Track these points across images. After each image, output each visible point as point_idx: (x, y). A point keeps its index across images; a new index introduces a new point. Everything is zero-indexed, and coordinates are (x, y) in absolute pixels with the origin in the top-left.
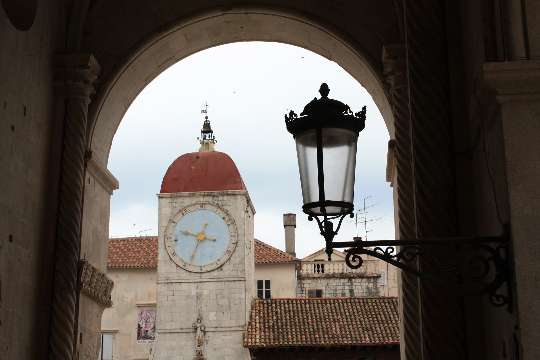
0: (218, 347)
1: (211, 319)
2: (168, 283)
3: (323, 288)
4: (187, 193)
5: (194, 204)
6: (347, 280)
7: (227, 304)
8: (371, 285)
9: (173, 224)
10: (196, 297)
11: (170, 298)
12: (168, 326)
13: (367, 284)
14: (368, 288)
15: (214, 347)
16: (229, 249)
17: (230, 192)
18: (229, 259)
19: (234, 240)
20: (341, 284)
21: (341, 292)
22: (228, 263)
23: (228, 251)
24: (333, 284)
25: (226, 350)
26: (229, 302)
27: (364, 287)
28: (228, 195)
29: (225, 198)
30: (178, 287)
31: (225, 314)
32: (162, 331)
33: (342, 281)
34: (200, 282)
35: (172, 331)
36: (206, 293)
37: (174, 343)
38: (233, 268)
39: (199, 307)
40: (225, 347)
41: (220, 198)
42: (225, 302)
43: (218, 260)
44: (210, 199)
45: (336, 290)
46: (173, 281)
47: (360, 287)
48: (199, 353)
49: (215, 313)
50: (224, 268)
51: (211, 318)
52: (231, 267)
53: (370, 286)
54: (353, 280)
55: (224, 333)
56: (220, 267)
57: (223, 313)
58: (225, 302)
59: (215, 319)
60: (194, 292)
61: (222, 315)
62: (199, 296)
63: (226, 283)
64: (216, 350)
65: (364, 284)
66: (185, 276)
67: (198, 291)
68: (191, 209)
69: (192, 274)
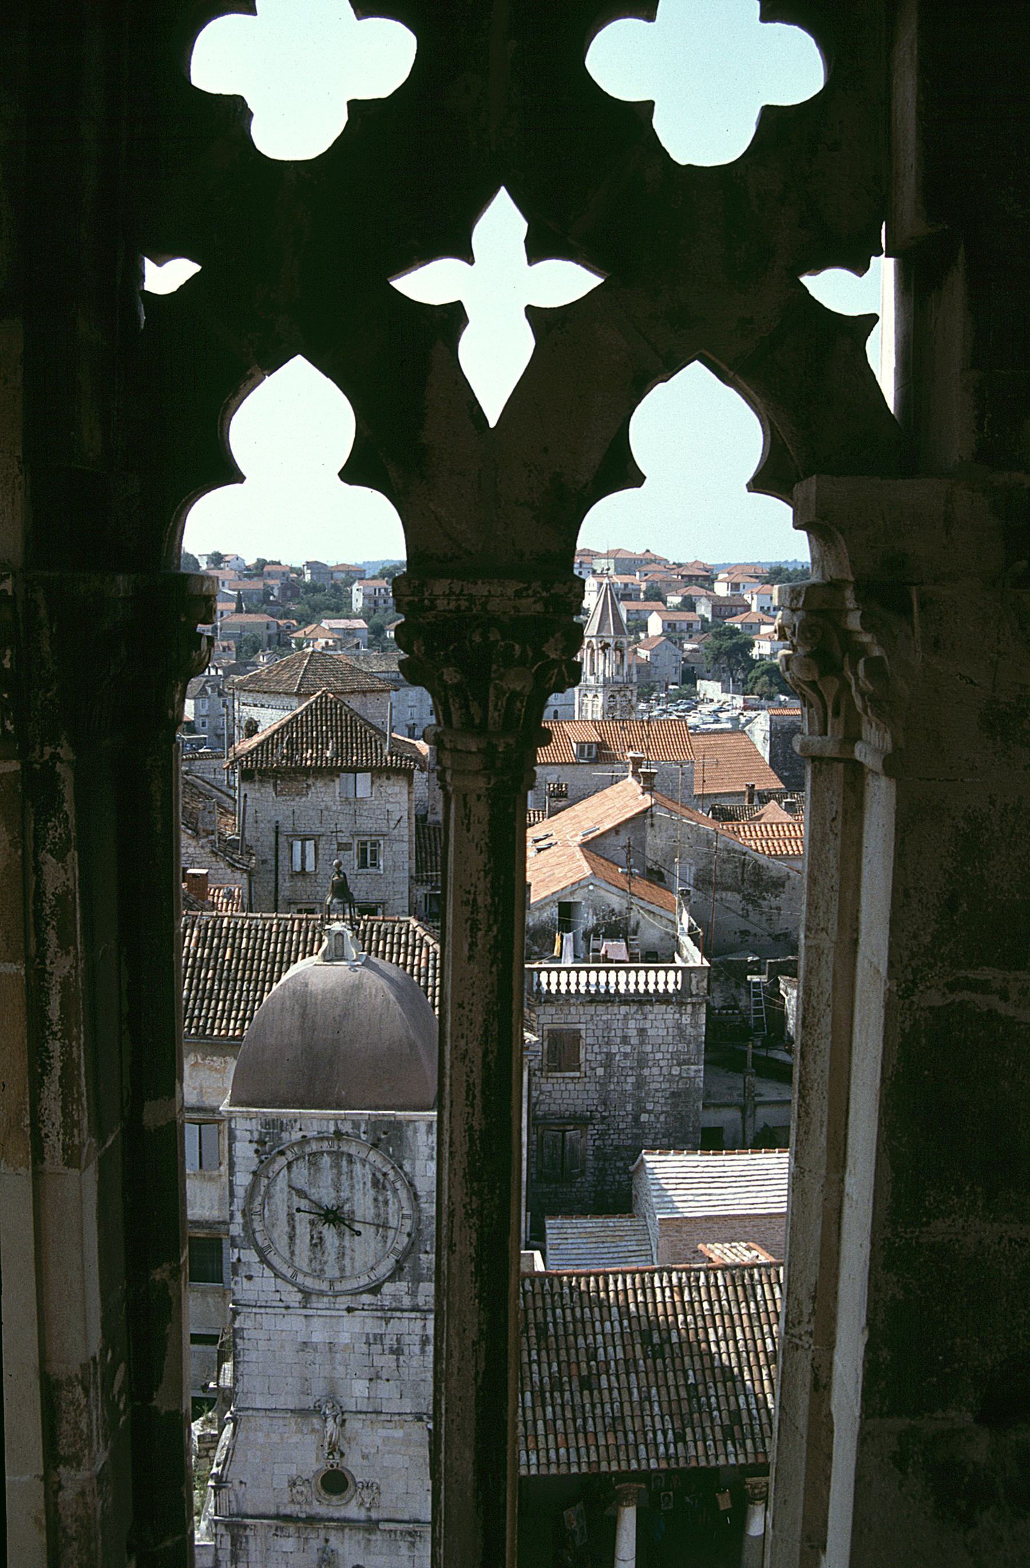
3: (582, 1026)
6: (634, 1008)
8: (686, 1020)
13: (677, 1016)
14: (679, 1027)
15: (364, 1450)
20: (622, 1017)
21: (619, 1033)
24: (604, 1018)
27: (670, 1023)
33: (624, 1009)
43: (372, 1269)
45: (609, 1029)
47: (660, 1024)
50: (388, 1288)
53: (684, 1022)
54: (648, 1008)
56: (375, 1290)
65: (671, 1016)
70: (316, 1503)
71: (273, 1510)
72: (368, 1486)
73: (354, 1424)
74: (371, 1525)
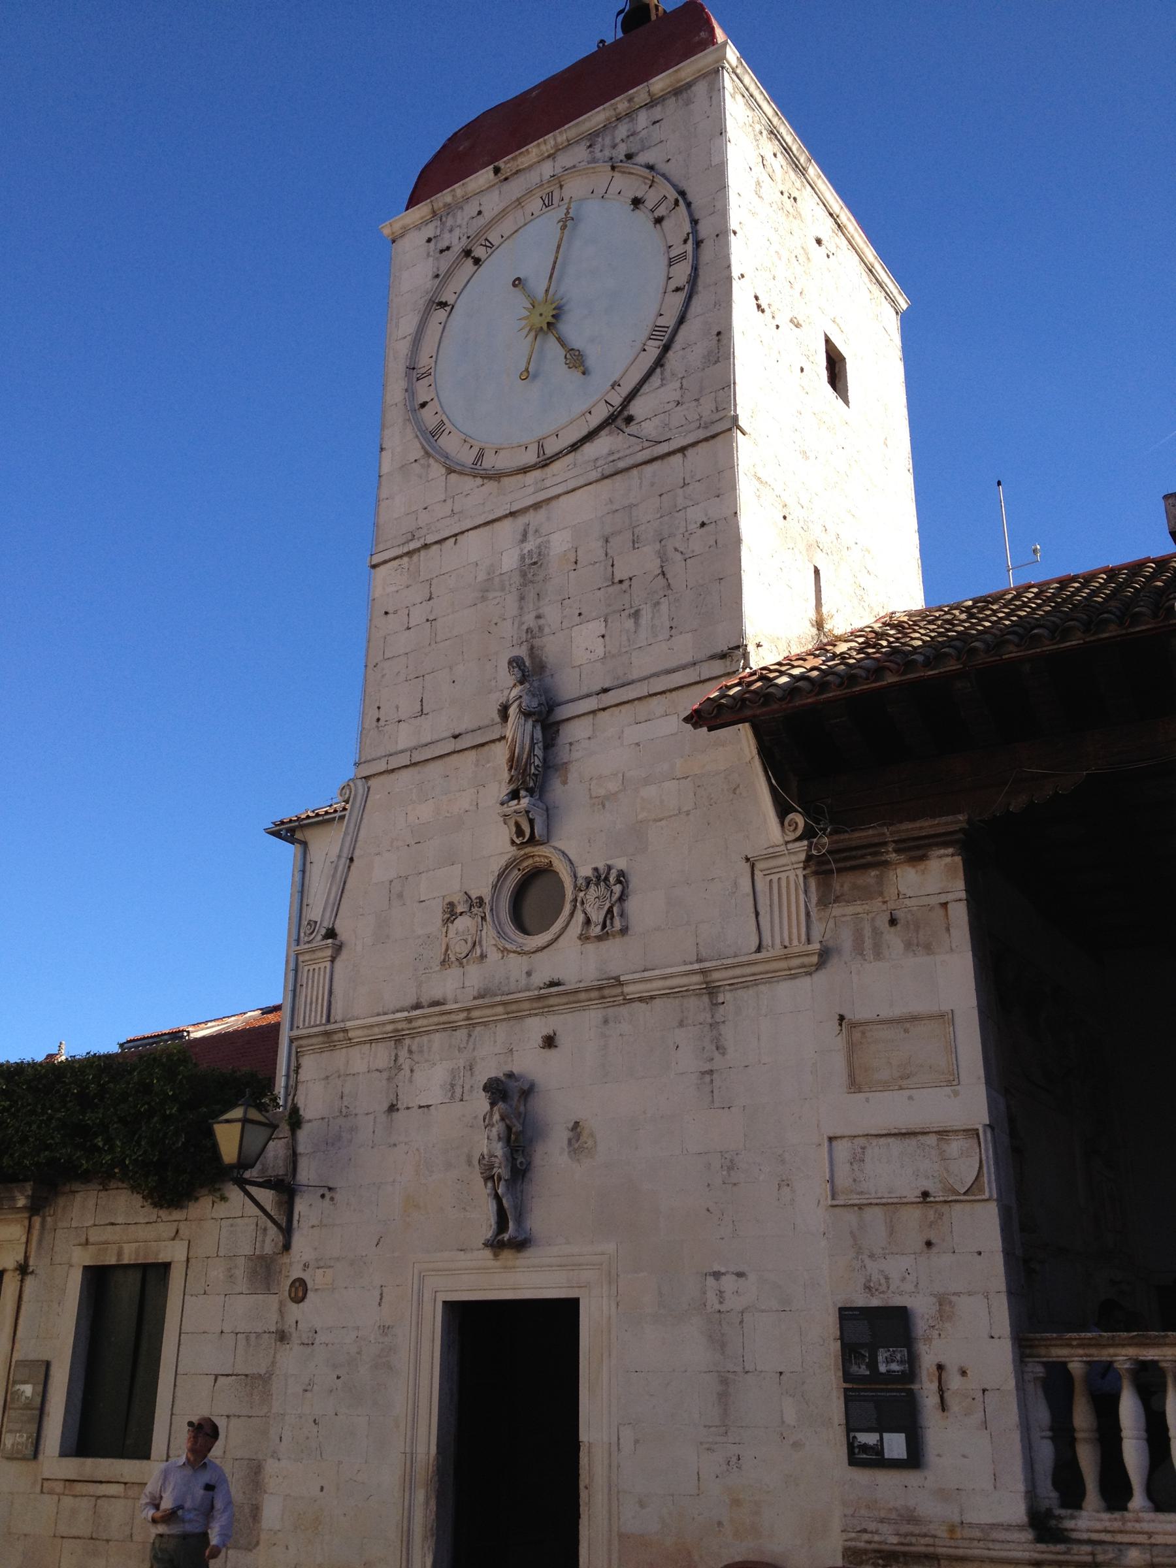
0: (613, 786)
1: (580, 656)
2: (409, 554)
4: (485, 176)
5: (519, 202)
7: (654, 566)
9: (442, 314)
10: (517, 579)
11: (418, 615)
12: (405, 737)
16: (661, 322)
17: (659, 83)
18: (659, 363)
19: (682, 272)
22: (655, 380)
23: (657, 328)
25: (650, 792)
26: (663, 557)
28: (653, 102)
29: (643, 119)
30: (448, 558)
31: (645, 619)
32: (382, 766)
34: (536, 506)
35: (417, 758)
36: (559, 543)
37: (424, 812)
38: (676, 396)
39: (529, 620)
40: (647, 781)
41: (622, 130)
42: (639, 563)
44: (580, 153)
46: (430, 539)
48: (520, 832)
49: (598, 627)
51: (580, 652)
52: (670, 392)
55: (641, 709)
57: (636, 615)
58: (639, 563)
59: (600, 652)
60: (510, 562)
61: (630, 624)
62: (532, 567)
63: (649, 469)
64: (602, 803)
66: (478, 499)
67: (529, 546)
68: (507, 226)
69: (506, 481)
70: (493, 956)
71: (411, 1000)
72: (600, 878)
73: (575, 732)
74: (608, 991)
